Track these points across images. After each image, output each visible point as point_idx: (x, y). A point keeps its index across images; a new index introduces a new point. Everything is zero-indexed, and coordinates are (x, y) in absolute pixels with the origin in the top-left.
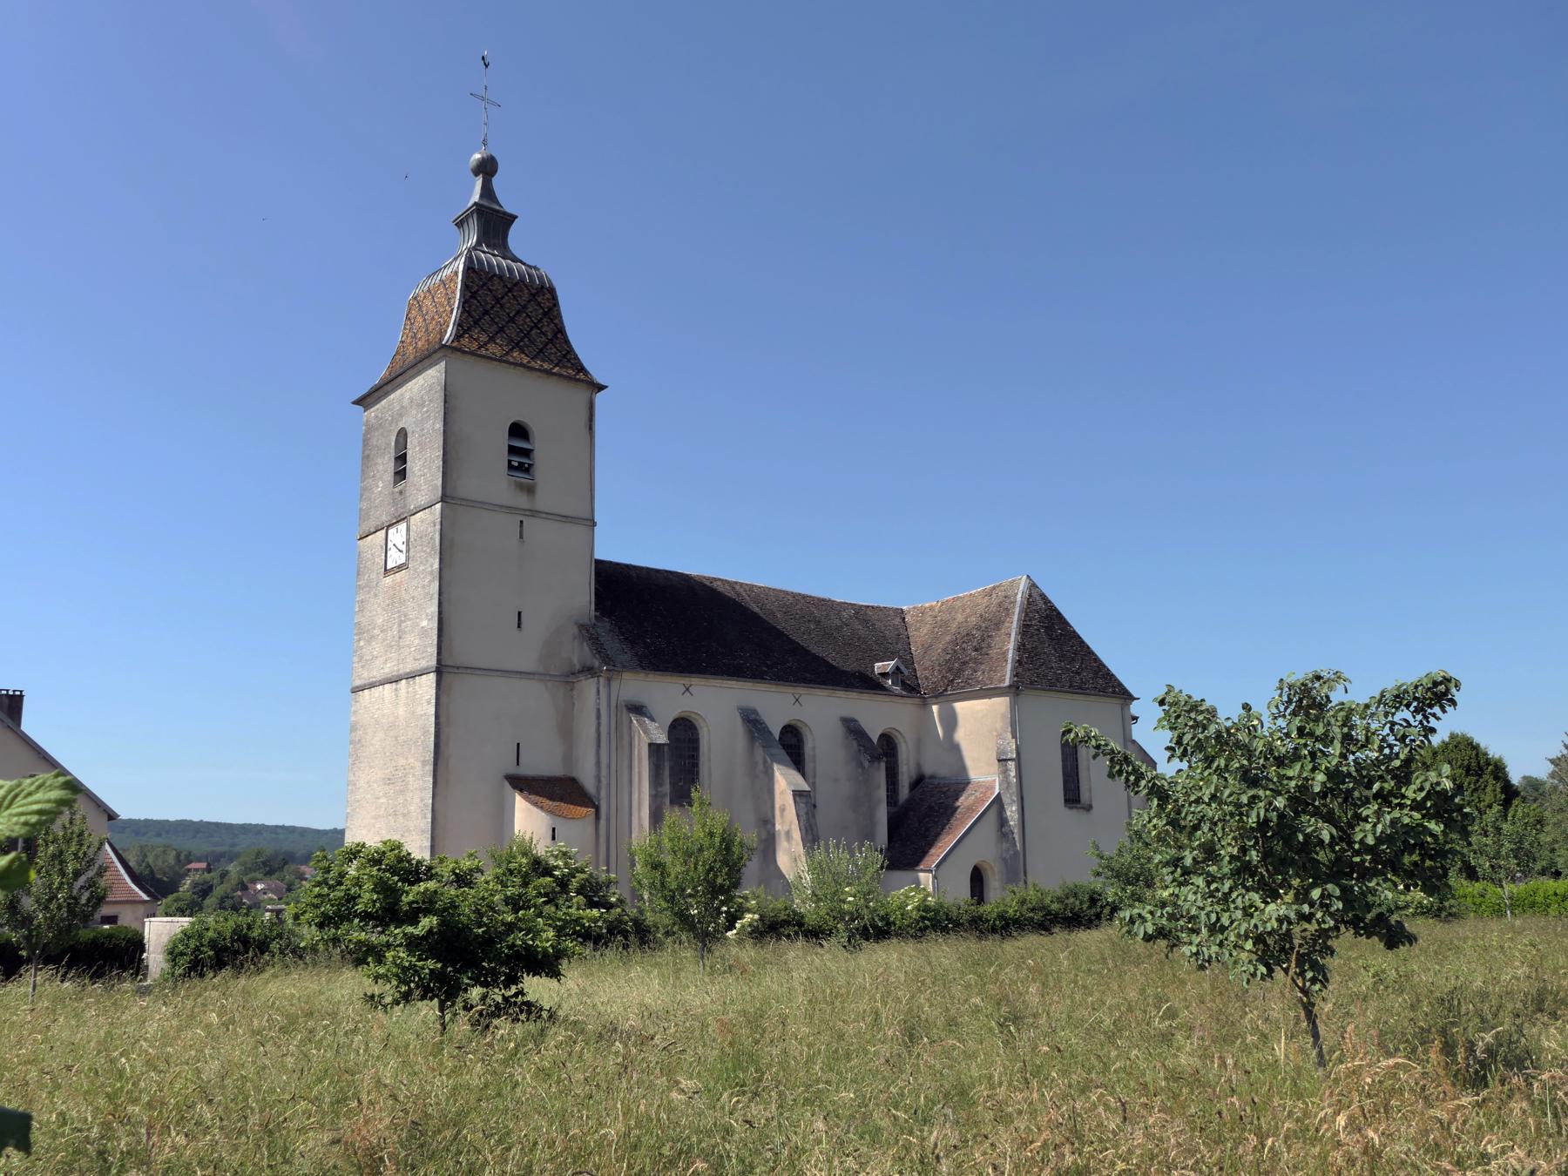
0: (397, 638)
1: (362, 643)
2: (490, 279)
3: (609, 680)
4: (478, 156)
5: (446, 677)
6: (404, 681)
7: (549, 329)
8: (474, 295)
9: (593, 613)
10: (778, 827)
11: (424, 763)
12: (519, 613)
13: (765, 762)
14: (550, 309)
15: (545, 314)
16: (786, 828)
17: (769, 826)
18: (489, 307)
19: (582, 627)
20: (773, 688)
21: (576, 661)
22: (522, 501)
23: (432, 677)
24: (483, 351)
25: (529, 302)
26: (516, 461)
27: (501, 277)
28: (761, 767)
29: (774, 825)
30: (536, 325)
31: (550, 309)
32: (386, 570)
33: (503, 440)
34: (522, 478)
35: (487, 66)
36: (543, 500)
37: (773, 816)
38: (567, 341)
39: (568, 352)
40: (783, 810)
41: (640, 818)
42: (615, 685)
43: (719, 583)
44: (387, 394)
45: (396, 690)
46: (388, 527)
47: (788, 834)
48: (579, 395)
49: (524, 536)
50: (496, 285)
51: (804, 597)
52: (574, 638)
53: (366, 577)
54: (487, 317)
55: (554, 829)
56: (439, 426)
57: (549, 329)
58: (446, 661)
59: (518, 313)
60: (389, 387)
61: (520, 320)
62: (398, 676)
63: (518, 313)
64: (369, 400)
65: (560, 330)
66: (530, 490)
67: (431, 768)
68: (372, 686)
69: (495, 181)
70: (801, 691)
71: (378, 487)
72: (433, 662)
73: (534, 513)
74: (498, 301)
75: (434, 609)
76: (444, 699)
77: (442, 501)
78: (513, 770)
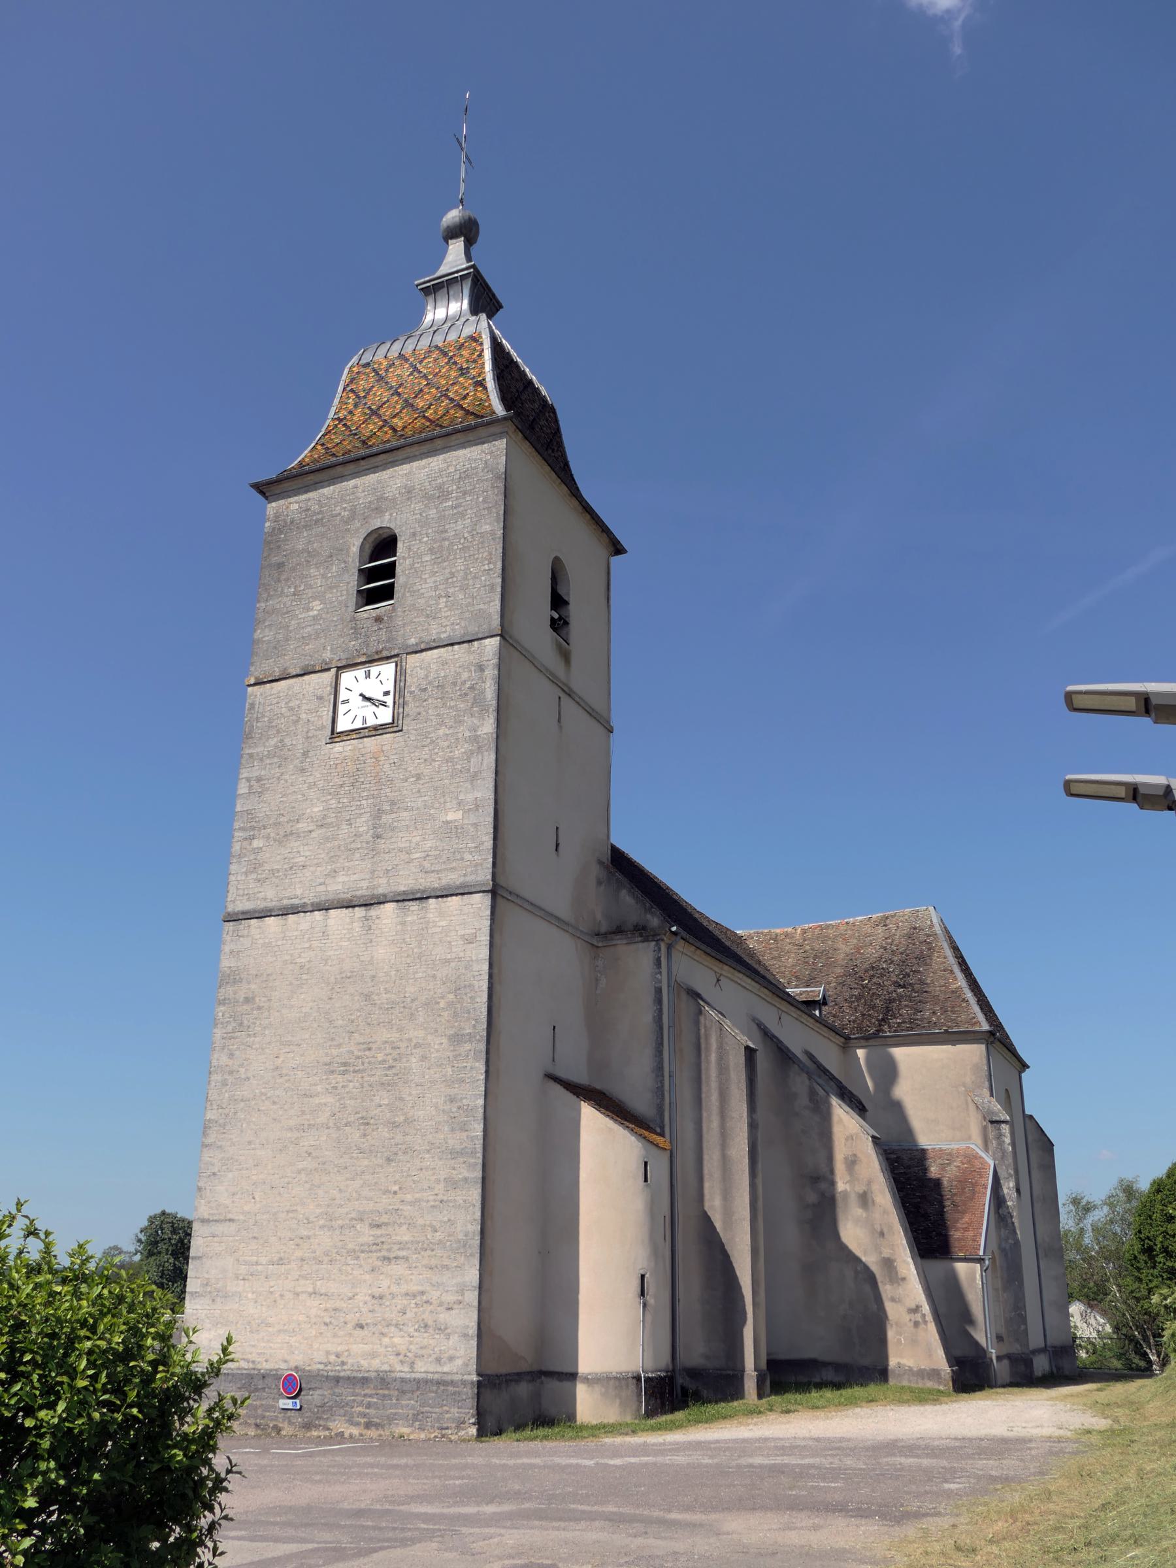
0: (369, 837)
1: (256, 843)
3: (669, 947)
6: (390, 906)
10: (841, 1186)
11: (457, 1039)
13: (812, 1093)
16: (860, 1189)
17: (823, 1186)
21: (599, 916)
23: (482, 903)
28: (803, 1100)
29: (833, 1183)
32: (333, 732)
37: (832, 1171)
40: (852, 1163)
41: (724, 1158)
44: (342, 478)
45: (366, 918)
46: (339, 668)
47: (865, 1199)
49: (562, 720)
52: (599, 883)
53: (273, 742)
55: (646, 1163)
56: (492, 526)
58: (501, 881)
60: (351, 468)
62: (373, 896)
64: (277, 489)
67: (482, 1046)
68: (262, 915)
71: (309, 609)
72: (484, 875)
75: (485, 791)
76: (497, 937)
77: (501, 635)
78: (551, 1070)
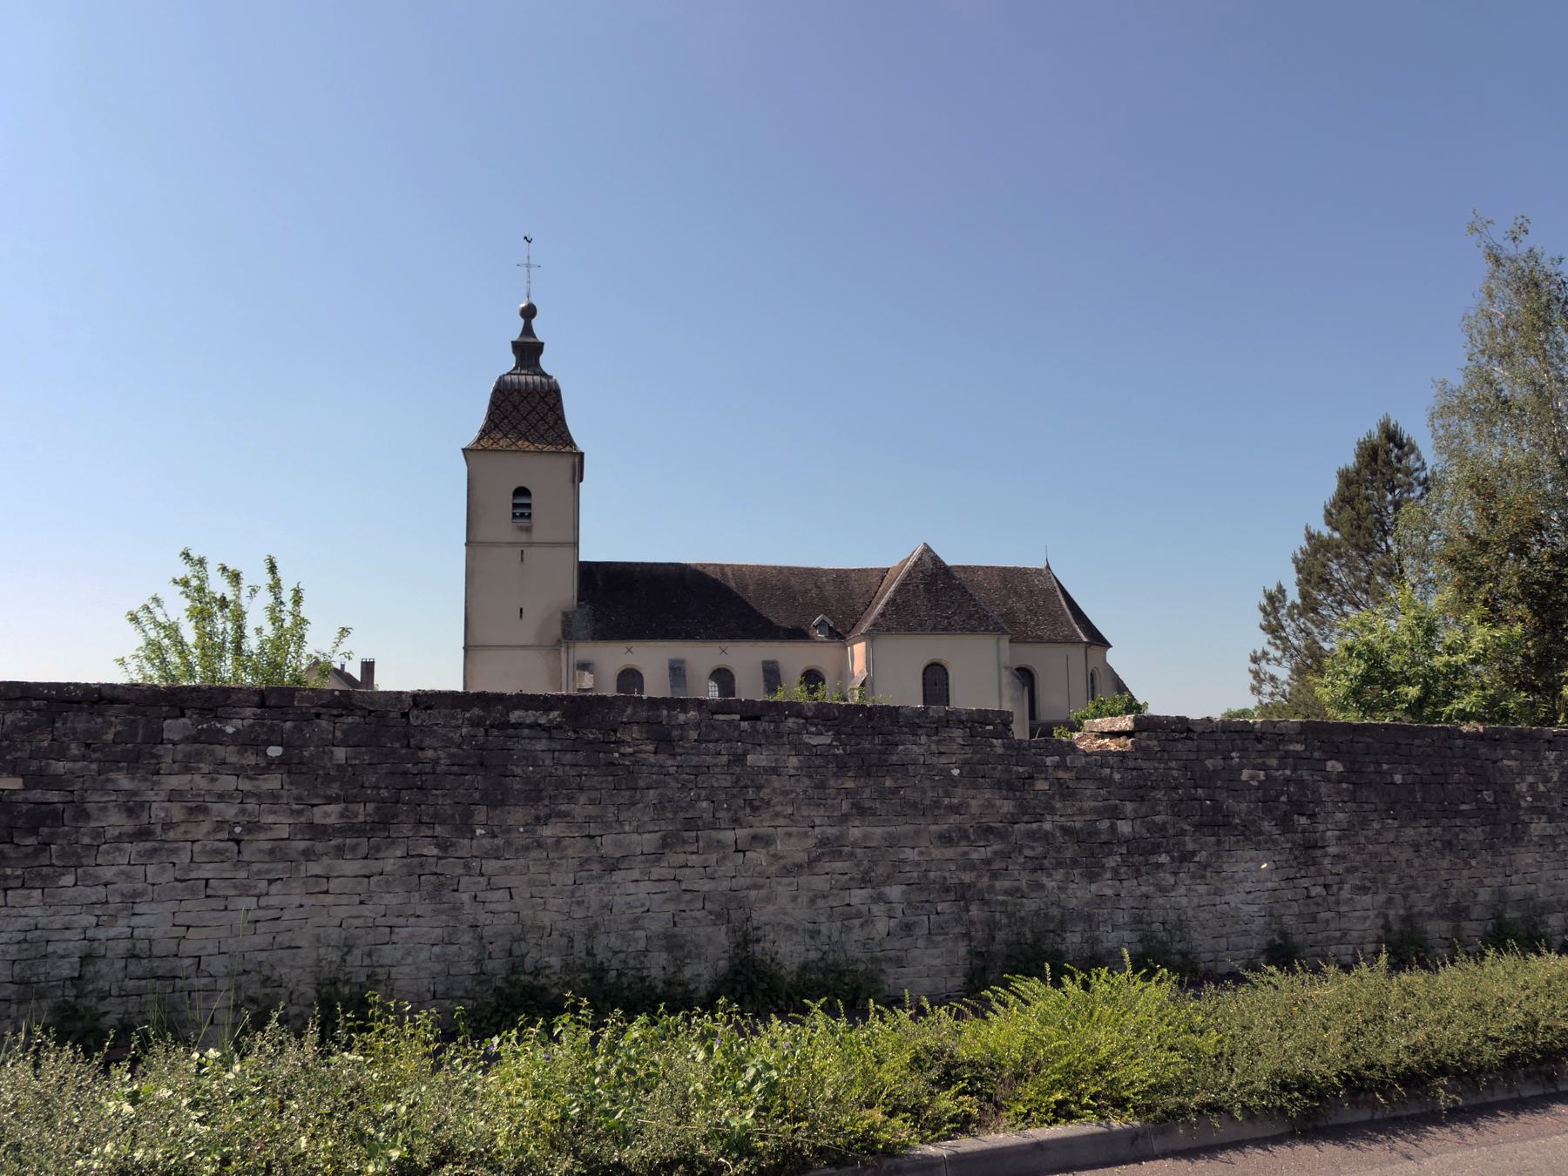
2: (512, 393)
4: (523, 305)
5: (471, 653)
7: (551, 418)
8: (498, 408)
9: (575, 603)
12: (521, 610)
14: (555, 404)
15: (550, 409)
18: (507, 413)
19: (565, 614)
20: (700, 644)
22: (523, 537)
24: (495, 446)
25: (538, 403)
26: (518, 511)
27: (519, 391)
30: (542, 419)
31: (555, 404)
33: (507, 500)
34: (524, 522)
35: (529, 242)
36: (537, 535)
38: (565, 425)
39: (563, 432)
42: (571, 651)
43: (712, 568)
48: (565, 464)
50: (516, 398)
51: (790, 569)
54: (506, 421)
57: (551, 421)
59: (530, 412)
61: (530, 418)
63: (530, 412)
65: (561, 418)
66: (528, 530)
69: (535, 322)
70: (725, 644)
73: (531, 544)
74: (515, 407)
